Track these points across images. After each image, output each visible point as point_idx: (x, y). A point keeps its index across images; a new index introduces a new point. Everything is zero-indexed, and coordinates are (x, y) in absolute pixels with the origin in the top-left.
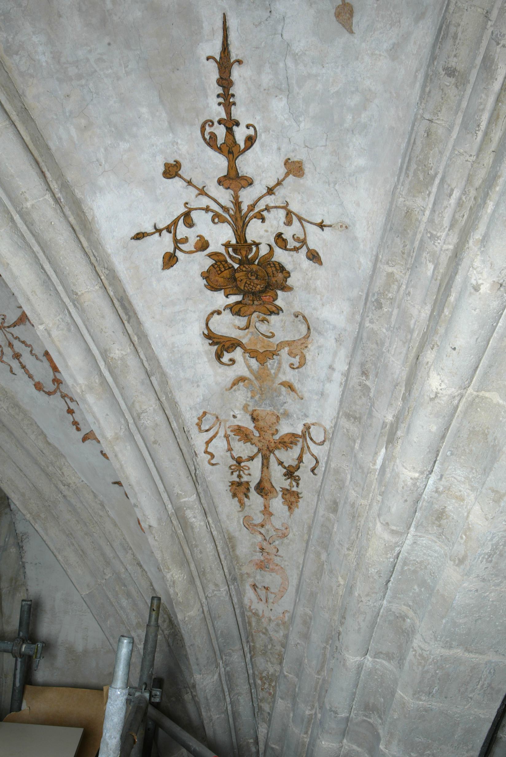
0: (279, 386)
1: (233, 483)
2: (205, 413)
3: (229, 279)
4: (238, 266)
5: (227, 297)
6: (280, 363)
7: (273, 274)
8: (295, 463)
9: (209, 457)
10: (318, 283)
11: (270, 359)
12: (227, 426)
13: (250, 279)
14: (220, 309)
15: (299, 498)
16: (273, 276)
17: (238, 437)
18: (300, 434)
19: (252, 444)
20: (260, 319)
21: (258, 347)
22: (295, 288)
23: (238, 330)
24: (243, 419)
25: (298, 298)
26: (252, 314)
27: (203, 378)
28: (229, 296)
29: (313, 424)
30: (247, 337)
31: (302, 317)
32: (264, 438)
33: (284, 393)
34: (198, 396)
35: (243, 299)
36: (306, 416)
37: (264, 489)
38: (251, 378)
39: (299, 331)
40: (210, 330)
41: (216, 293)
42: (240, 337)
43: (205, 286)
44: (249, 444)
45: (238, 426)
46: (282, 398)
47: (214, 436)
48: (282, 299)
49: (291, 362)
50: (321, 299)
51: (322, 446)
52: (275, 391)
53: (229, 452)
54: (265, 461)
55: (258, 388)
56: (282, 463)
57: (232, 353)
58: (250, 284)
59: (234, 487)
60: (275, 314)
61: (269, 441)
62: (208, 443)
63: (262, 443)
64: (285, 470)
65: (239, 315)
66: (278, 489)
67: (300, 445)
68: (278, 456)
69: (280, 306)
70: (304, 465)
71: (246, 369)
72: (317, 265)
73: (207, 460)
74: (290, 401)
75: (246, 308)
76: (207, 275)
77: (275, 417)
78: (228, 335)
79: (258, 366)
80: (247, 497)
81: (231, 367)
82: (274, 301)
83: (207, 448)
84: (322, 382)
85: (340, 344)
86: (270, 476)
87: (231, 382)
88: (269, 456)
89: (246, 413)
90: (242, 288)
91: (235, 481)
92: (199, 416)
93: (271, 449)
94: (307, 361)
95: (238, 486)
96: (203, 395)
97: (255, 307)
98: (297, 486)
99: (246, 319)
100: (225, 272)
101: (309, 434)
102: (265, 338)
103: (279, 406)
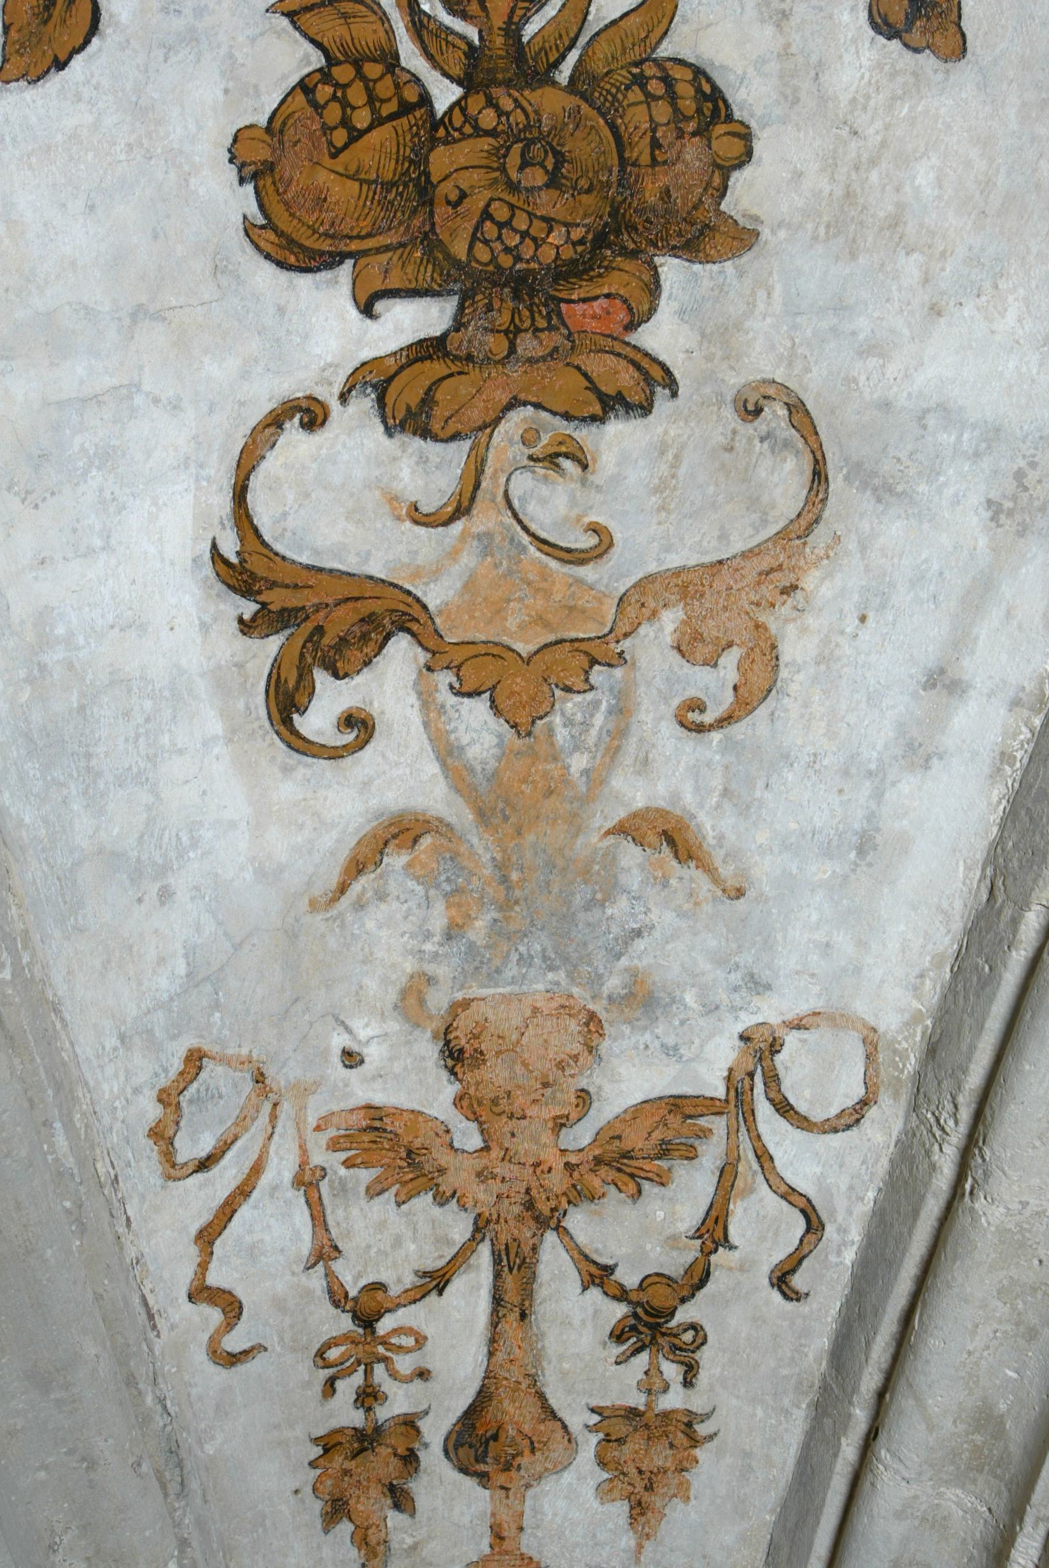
0: (611, 840)
1: (329, 1444)
2: (195, 1060)
3: (389, 186)
4: (456, 92)
5: (367, 310)
6: (622, 710)
7: (655, 144)
8: (676, 1262)
9: (215, 1316)
10: (923, 177)
11: (568, 689)
12: (312, 1121)
13: (513, 187)
14: (321, 393)
15: (695, 1441)
16: (654, 162)
17: (365, 1176)
18: (720, 1092)
19: (441, 1200)
20: (537, 451)
21: (512, 623)
22: (766, 233)
23: (408, 524)
24: (397, 1067)
25: (777, 295)
26: (497, 421)
27: (195, 843)
28: (379, 306)
29: (798, 1025)
30: (456, 569)
31: (783, 412)
32: (507, 1156)
33: (633, 880)
34: (161, 961)
35: (458, 324)
36: (757, 985)
37: (495, 1437)
38: (453, 820)
39: (753, 503)
40: (256, 530)
41: (304, 281)
42: (416, 574)
43: (249, 229)
44: (425, 1200)
45: (369, 1107)
46: (619, 908)
47: (243, 1192)
48: (681, 313)
49: (691, 692)
50: (926, 281)
51: (853, 1133)
52: (586, 873)
53: (320, 1268)
54: (509, 1281)
55: (487, 872)
56: (609, 1270)
57: (358, 679)
58: (508, 224)
59: (338, 1461)
60: (629, 407)
61: (536, 1165)
62: (207, 1237)
63: (496, 1186)
64: (620, 1310)
65: (425, 433)
66: (577, 1419)
67: (711, 1155)
68: (581, 1239)
69: (663, 358)
70: (736, 1254)
71: (432, 768)
72: (927, 60)
73: (205, 1337)
74: (663, 918)
75: (463, 386)
76: (263, 153)
77: (573, 1026)
78: (350, 563)
79: (499, 745)
80: (401, 1499)
81: (349, 760)
82: (632, 326)
83: (203, 1267)
84: (870, 773)
85: (1022, 533)
86: (538, 1358)
87: (343, 855)
88: (534, 1249)
89: (417, 1025)
90: (460, 249)
91: (340, 1431)
92: (163, 1082)
93: (544, 1208)
94: (784, 673)
95: (354, 1456)
96: (190, 952)
97: (515, 372)
98: (688, 1383)
99: (459, 451)
100: (375, 136)
101: (772, 1079)
102: (553, 564)
103: (600, 960)
